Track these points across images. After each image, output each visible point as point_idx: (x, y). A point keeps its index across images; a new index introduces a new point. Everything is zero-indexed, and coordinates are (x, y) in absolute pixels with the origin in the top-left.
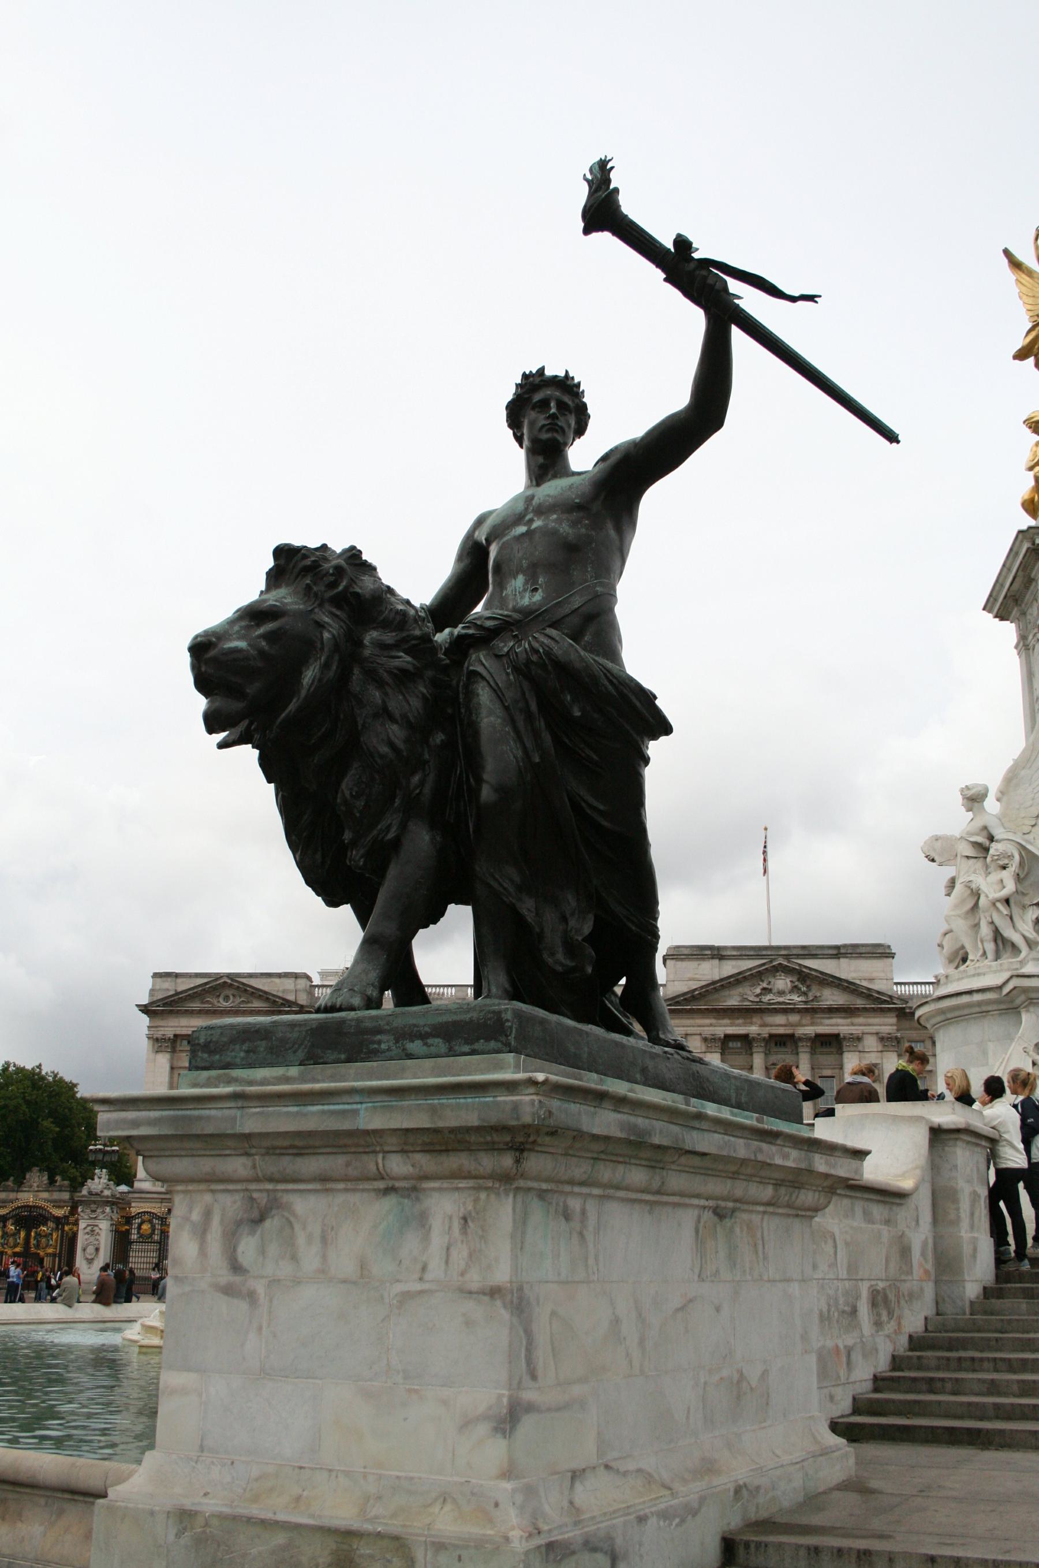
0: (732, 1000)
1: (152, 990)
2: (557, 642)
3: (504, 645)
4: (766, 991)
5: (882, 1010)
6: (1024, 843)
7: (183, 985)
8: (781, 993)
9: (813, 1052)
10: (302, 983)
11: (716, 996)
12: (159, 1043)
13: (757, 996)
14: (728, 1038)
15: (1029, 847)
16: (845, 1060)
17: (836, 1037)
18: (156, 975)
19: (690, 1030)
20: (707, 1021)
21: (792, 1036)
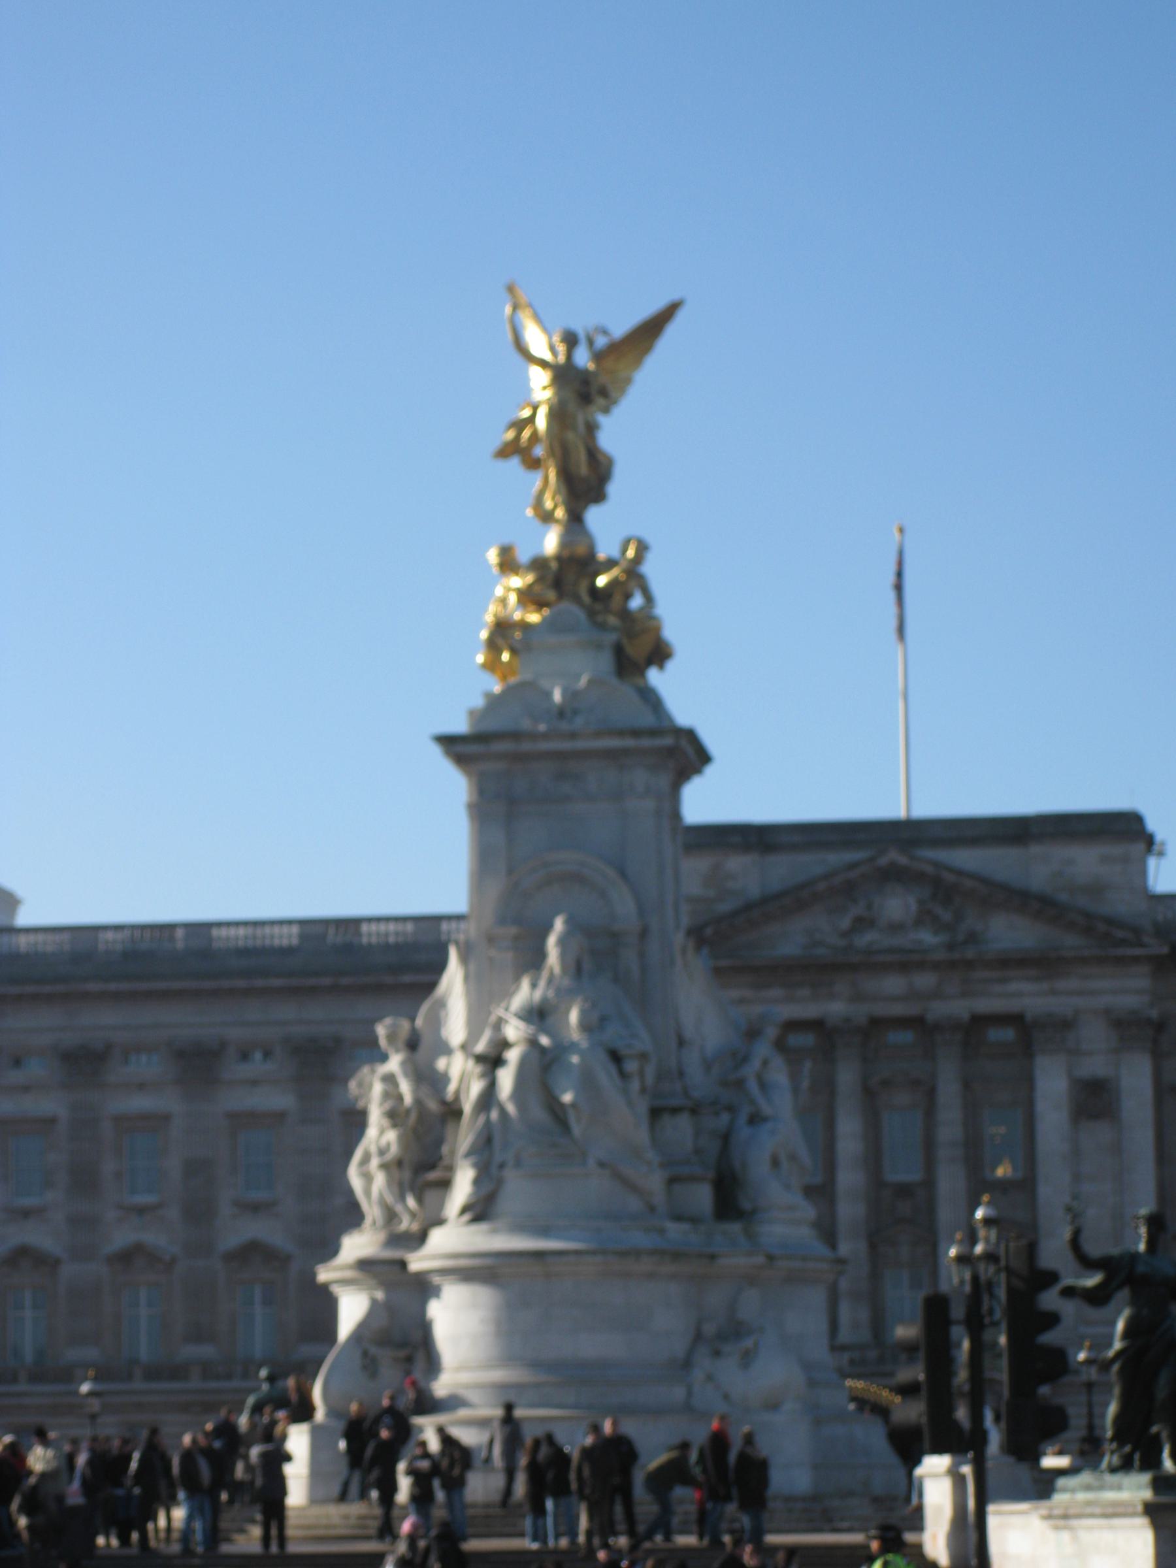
0: (790, 939)
4: (863, 923)
5: (1120, 961)
8: (896, 928)
13: (845, 934)
17: (1015, 1020)
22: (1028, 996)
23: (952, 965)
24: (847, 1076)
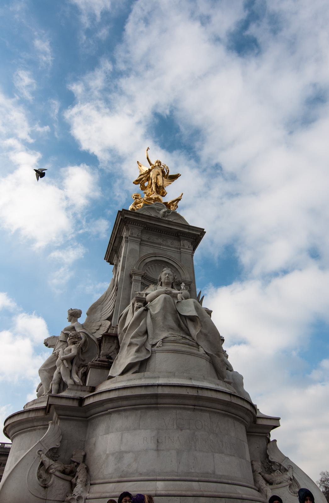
6: (89, 334)
15: (91, 337)
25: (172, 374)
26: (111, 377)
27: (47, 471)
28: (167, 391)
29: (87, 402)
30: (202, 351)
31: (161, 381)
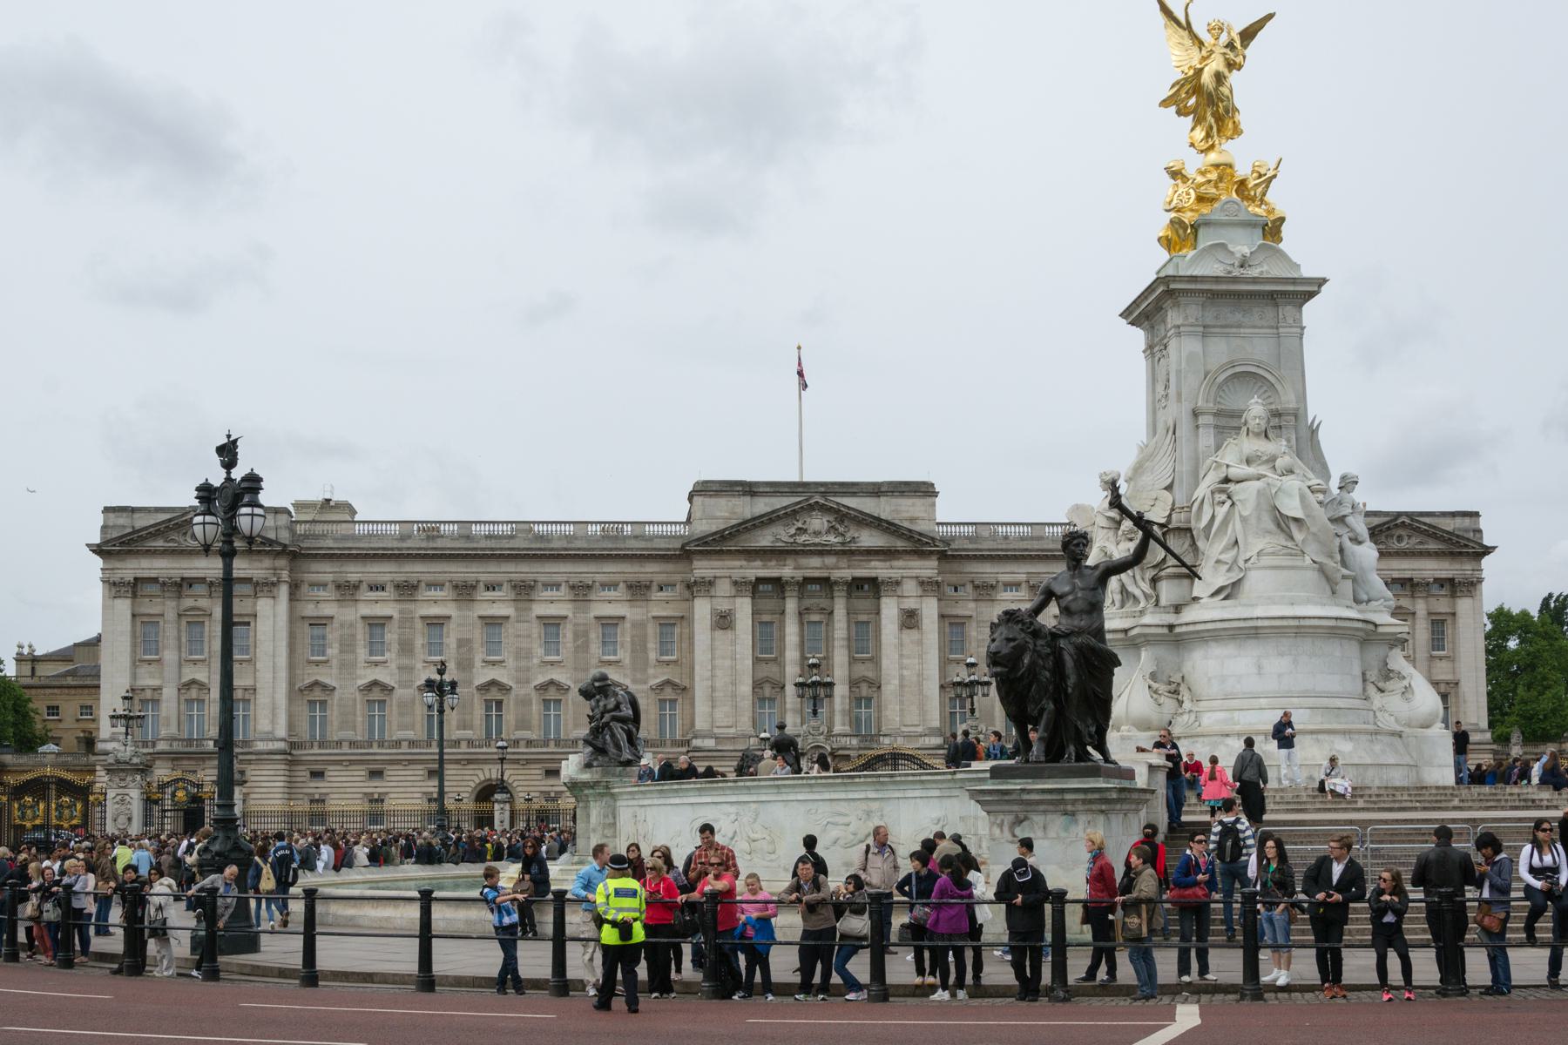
0: (764, 539)
1: (104, 528)
2: (1093, 641)
3: (1074, 639)
4: (801, 531)
7: (142, 522)
8: (817, 533)
9: (849, 596)
10: (283, 520)
11: (747, 536)
12: (114, 587)
14: (760, 580)
16: (883, 606)
17: (873, 581)
18: (107, 510)
19: (718, 573)
20: (737, 563)
21: (827, 580)
22: (878, 569)
23: (844, 552)
24: (791, 605)
25: (1272, 601)
26: (1195, 599)
27: (1156, 692)
28: (1266, 623)
29: (1178, 630)
30: (1308, 561)
31: (1259, 612)
